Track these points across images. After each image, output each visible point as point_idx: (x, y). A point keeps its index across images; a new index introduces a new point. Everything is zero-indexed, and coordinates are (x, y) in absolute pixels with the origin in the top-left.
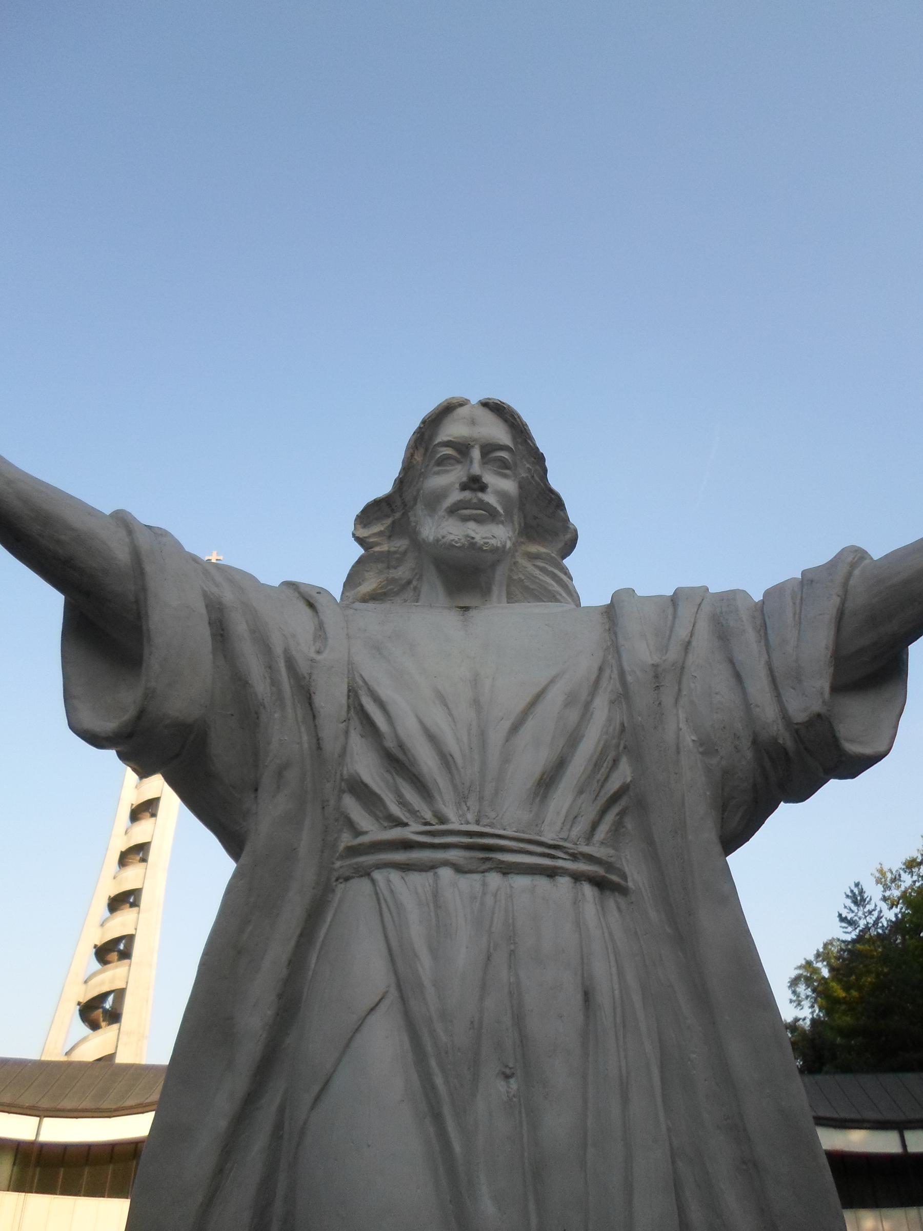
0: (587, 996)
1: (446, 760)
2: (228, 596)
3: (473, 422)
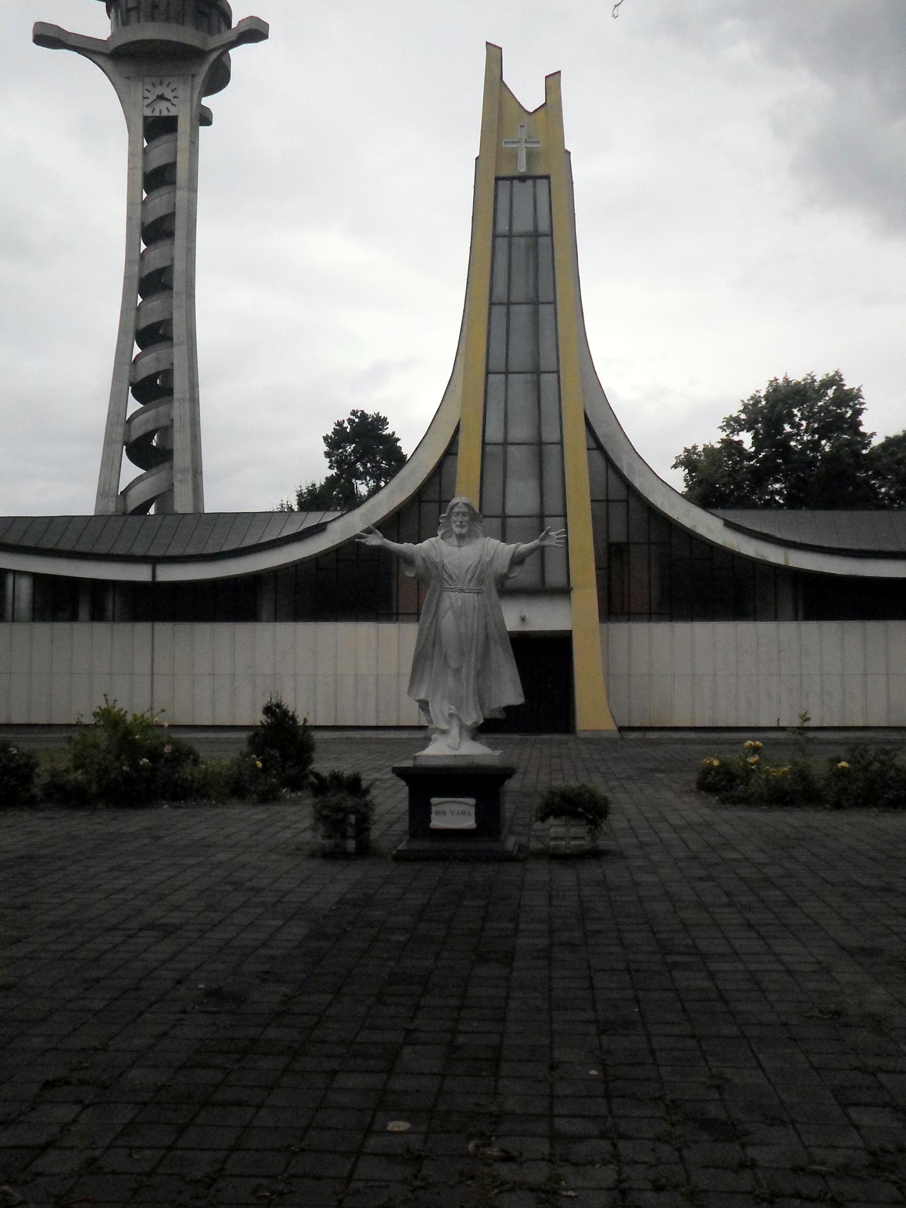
0: (474, 607)
1: (457, 577)
2: (424, 555)
3: (460, 508)
